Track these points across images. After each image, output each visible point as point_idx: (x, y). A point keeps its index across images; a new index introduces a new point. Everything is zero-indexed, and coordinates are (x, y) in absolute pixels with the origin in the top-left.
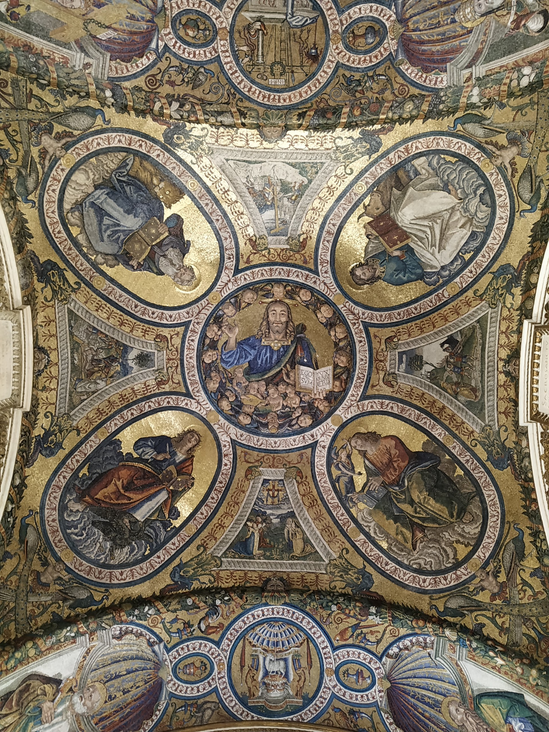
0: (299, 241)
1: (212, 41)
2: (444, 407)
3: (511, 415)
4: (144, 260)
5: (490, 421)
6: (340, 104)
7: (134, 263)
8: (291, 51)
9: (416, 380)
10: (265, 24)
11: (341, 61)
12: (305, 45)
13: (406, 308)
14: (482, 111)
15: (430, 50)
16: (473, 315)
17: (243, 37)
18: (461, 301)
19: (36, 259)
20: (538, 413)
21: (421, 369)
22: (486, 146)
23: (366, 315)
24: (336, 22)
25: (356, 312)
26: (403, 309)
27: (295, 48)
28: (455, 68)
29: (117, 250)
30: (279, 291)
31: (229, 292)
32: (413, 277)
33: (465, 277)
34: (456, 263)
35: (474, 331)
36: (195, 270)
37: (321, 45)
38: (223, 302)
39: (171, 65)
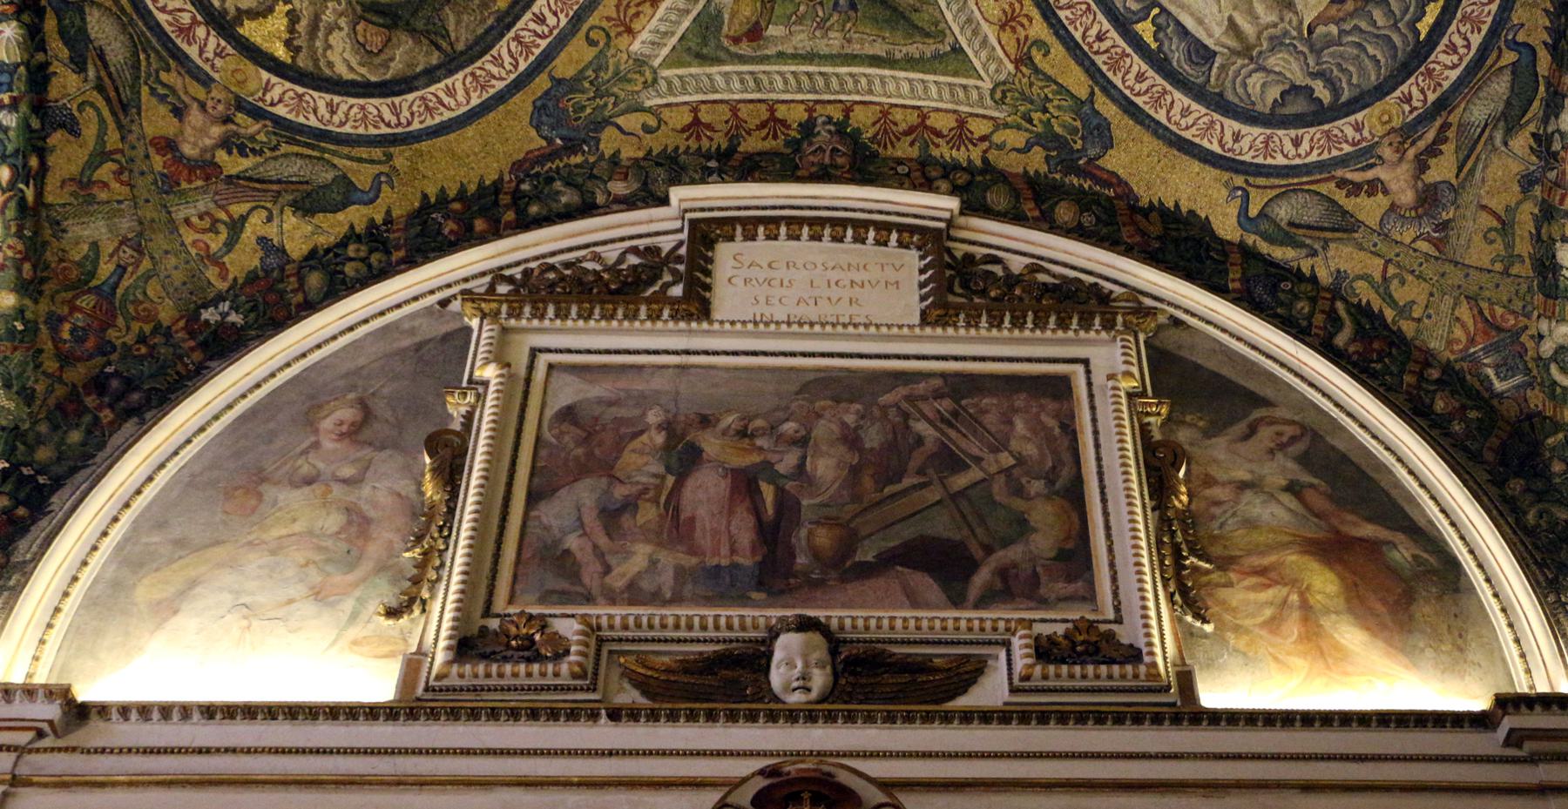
5: (669, 83)
14: (1532, 128)
16: (975, 32)
20: (710, 244)
22: (1438, 123)
33: (1087, 20)
35: (928, 35)
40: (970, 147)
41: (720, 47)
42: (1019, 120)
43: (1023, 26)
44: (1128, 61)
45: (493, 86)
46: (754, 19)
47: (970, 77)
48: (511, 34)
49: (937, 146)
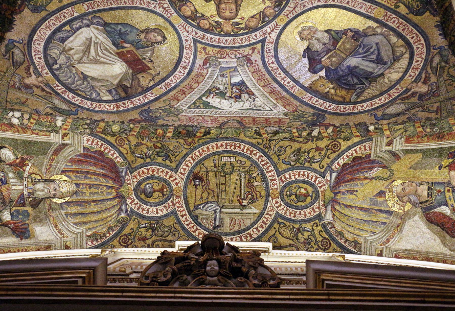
0: (210, 64)
1: (284, 187)
4: (341, 38)
6: (174, 140)
7: (350, 34)
8: (217, 183)
10: (239, 204)
11: (173, 173)
12: (204, 188)
13: (119, 6)
15: (98, 168)
17: (258, 193)
19: (432, 12)
23: (153, 6)
24: (178, 205)
25: (161, 9)
26: (122, 5)
27: (213, 186)
28: (76, 147)
29: (365, 40)
30: (227, 28)
31: (270, 25)
32: (113, 27)
34: (77, 26)
36: (299, 39)
37: (191, 188)
38: (275, 17)
39: (318, 164)
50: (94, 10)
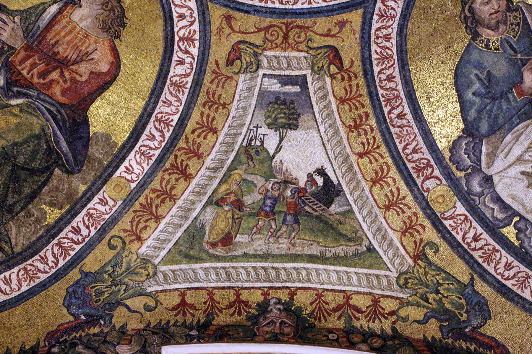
2: (188, 177)
3: (181, 320)
5: (165, 276)
9: (245, 115)
13: (402, 95)
16: (384, 238)
18: (415, 214)
21: (269, 126)
26: (400, 87)
32: (472, 114)
34: (496, 208)
35: (350, 240)
40: (383, 320)
41: (202, 250)
42: (419, 300)
43: (418, 232)
44: (498, 255)
45: (39, 278)
46: (227, 230)
47: (381, 268)
48: (55, 241)
49: (358, 319)
50: (432, 163)
